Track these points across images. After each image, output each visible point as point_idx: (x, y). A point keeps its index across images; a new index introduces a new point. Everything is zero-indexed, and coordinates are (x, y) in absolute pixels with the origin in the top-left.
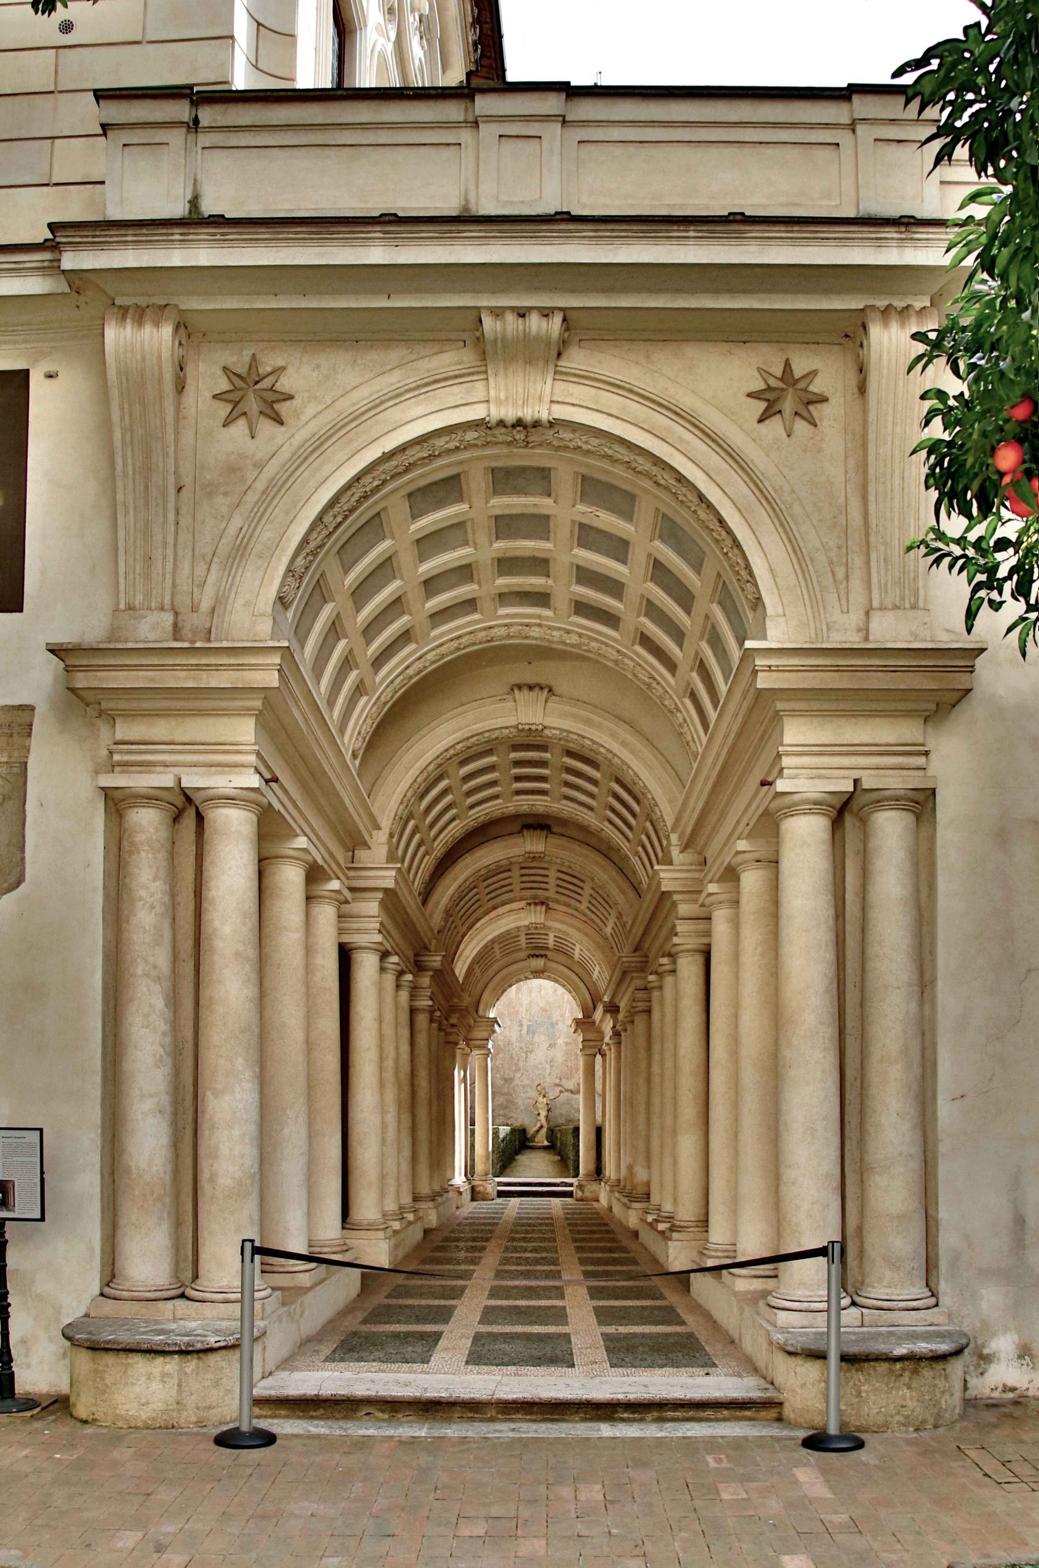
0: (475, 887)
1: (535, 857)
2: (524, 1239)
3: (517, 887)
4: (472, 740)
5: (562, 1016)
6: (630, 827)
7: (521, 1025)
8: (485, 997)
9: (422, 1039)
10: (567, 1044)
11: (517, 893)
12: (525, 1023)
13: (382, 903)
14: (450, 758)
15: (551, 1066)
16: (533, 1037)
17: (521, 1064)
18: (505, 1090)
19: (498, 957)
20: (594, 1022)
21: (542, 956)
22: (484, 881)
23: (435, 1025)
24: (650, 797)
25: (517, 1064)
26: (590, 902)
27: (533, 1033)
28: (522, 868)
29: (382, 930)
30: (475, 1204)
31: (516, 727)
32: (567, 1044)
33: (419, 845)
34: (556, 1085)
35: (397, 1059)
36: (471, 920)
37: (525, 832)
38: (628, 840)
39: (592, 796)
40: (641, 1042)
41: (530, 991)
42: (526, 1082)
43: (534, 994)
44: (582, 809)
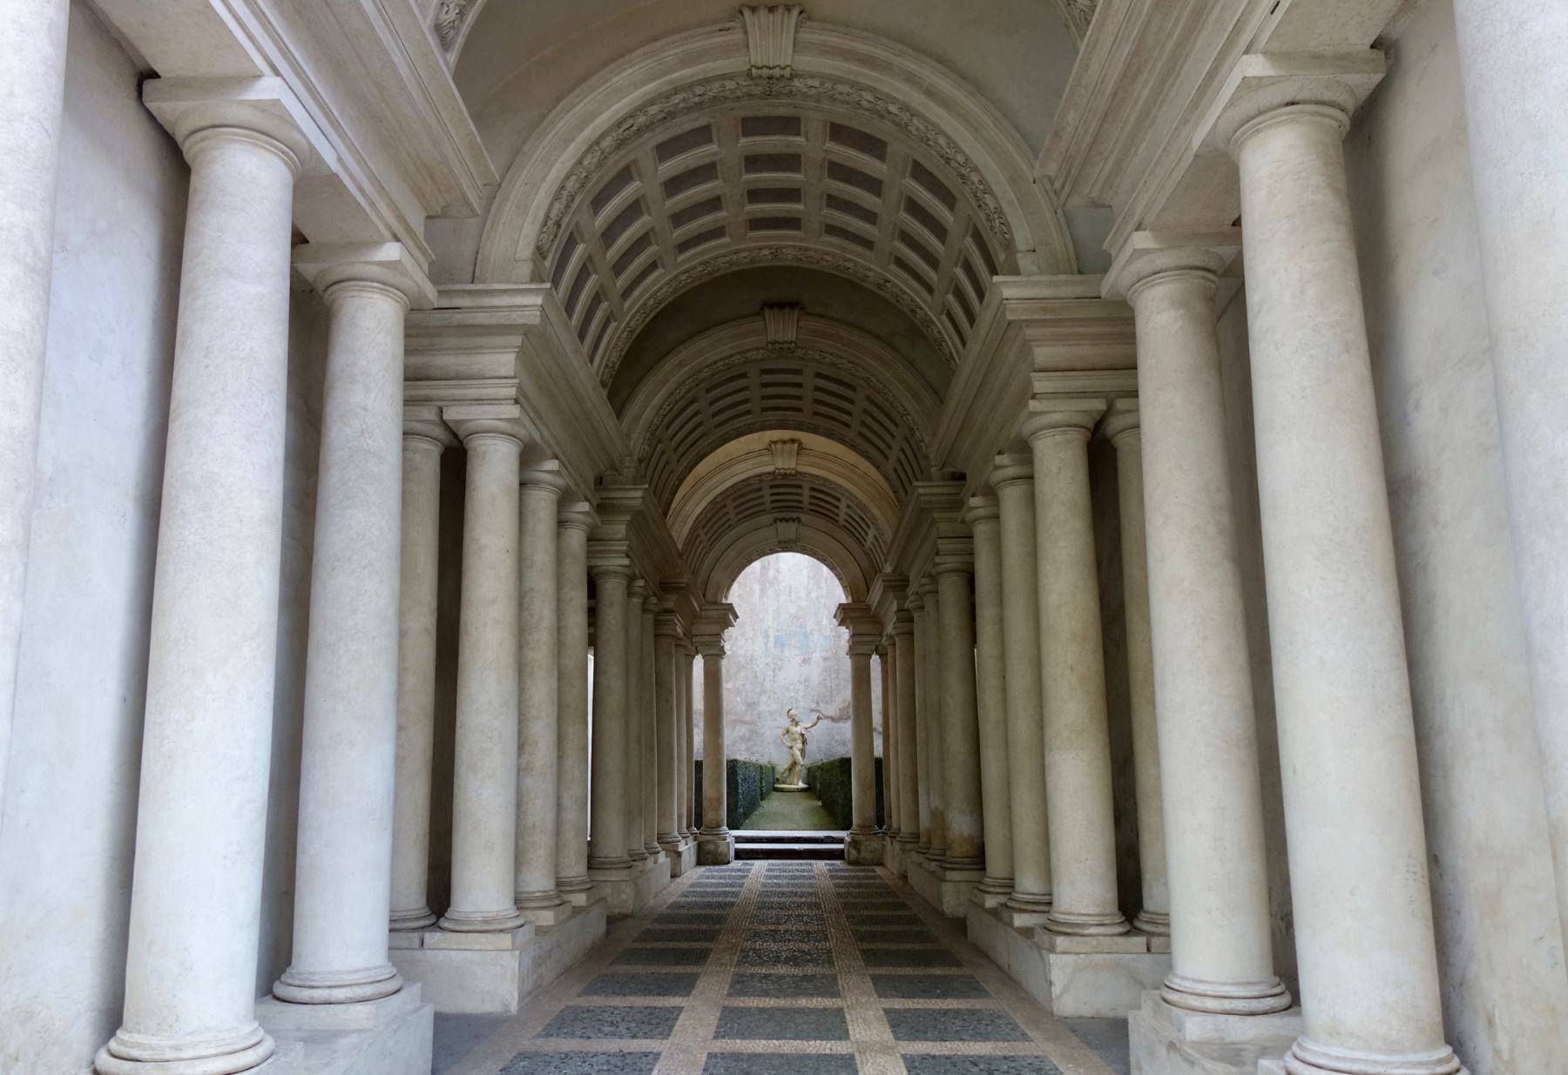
0: (693, 401)
1: (783, 350)
2: (774, 935)
4: (677, 99)
5: (819, 624)
6: (933, 261)
7: (767, 636)
9: (612, 617)
10: (825, 659)
12: (772, 634)
13: (523, 356)
14: (639, 132)
15: (806, 687)
17: (767, 684)
18: (747, 718)
20: (869, 608)
22: (708, 391)
23: (636, 601)
24: (975, 178)
26: (863, 423)
27: (783, 645)
28: (764, 372)
29: (522, 400)
30: (702, 869)
31: (749, 75)
32: (825, 659)
33: (596, 300)
35: (559, 630)
36: (691, 455)
37: (767, 312)
38: (930, 290)
39: (870, 217)
40: (952, 616)
41: (777, 596)
42: (774, 707)
43: (782, 598)
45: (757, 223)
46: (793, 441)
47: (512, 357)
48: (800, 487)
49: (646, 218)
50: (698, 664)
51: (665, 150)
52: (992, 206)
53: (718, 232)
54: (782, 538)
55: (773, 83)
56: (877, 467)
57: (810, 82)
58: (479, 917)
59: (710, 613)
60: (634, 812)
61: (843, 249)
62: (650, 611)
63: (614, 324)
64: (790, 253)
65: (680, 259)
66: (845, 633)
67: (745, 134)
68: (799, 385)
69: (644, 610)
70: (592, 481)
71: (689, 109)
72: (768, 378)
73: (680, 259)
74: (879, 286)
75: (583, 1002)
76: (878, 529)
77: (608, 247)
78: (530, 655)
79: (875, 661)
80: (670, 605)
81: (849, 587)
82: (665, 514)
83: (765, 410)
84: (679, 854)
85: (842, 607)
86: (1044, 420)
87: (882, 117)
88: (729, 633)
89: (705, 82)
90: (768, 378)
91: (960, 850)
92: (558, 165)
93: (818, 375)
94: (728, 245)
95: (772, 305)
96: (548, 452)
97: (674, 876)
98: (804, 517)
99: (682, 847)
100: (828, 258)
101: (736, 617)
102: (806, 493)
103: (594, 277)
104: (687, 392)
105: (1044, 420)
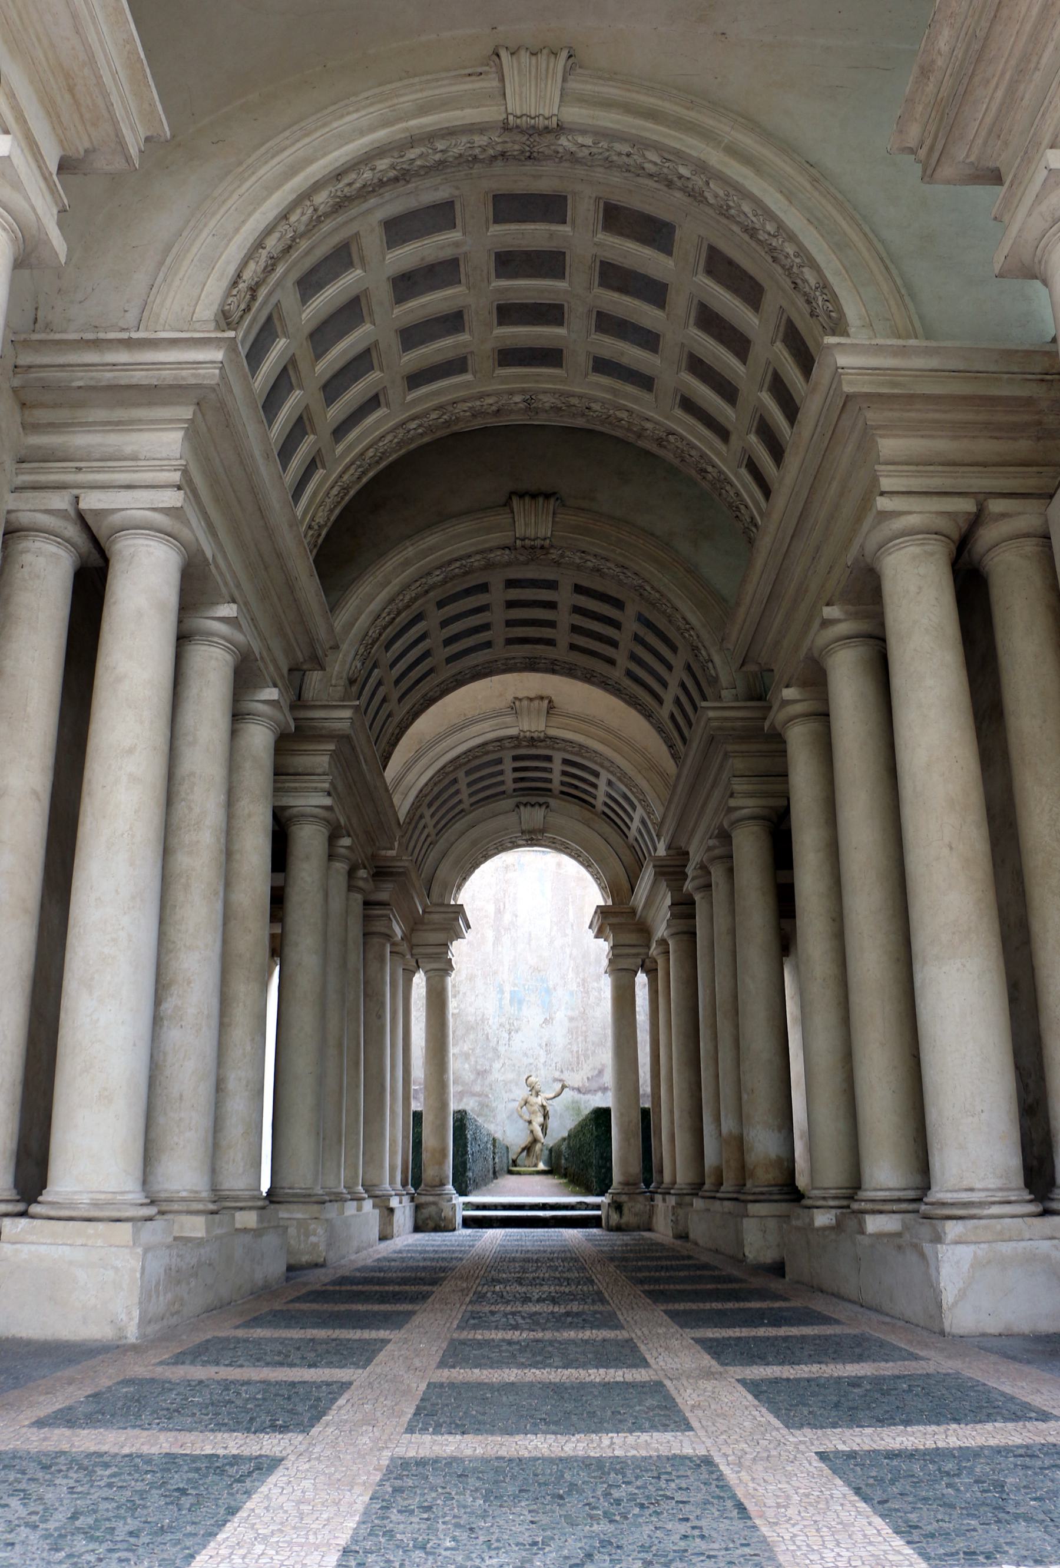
0: (419, 617)
1: (536, 551)
3: (498, 633)
8: (441, 873)
11: (499, 651)
15: (548, 1052)
16: (520, 1009)
17: (502, 1049)
18: (477, 1088)
19: (465, 805)
20: (633, 912)
21: (540, 805)
22: (441, 604)
23: (341, 867)
25: (495, 1050)
26: (633, 657)
28: (511, 584)
30: (419, 1236)
34: (556, 1080)
37: (515, 501)
38: (724, 434)
39: (650, 340)
42: (510, 1076)
44: (630, 389)
45: (508, 356)
46: (542, 698)
47: (179, 435)
48: (549, 758)
49: (367, 328)
50: (419, 981)
51: (398, 230)
52: (813, 282)
53: (456, 365)
54: (524, 828)
55: (532, 139)
56: (648, 715)
57: (580, 140)
58: (85, 1199)
59: (435, 917)
60: (329, 1138)
61: (614, 392)
62: (360, 890)
63: (320, 473)
64: (548, 400)
65: (409, 398)
66: (603, 947)
67: (496, 221)
68: (552, 605)
69: (351, 888)
70: (285, 671)
71: (429, 170)
72: (515, 594)
73: (409, 398)
74: (660, 442)
75: (241, 1333)
76: (646, 807)
77: (318, 357)
78: (183, 860)
79: (641, 979)
80: (383, 896)
81: (611, 888)
82: (384, 768)
83: (510, 641)
84: (391, 1210)
85: (602, 912)
86: (898, 524)
87: (670, 184)
88: (458, 950)
89: (450, 132)
90: (515, 594)
91: (764, 1177)
92: (257, 215)
93: (579, 589)
94: (467, 385)
95: (521, 496)
96: (224, 590)
97: (383, 1238)
98: (552, 802)
99: (394, 1203)
100: (595, 406)
101: (468, 927)
102: (557, 766)
103: (297, 394)
104: (414, 600)
105: (898, 524)
